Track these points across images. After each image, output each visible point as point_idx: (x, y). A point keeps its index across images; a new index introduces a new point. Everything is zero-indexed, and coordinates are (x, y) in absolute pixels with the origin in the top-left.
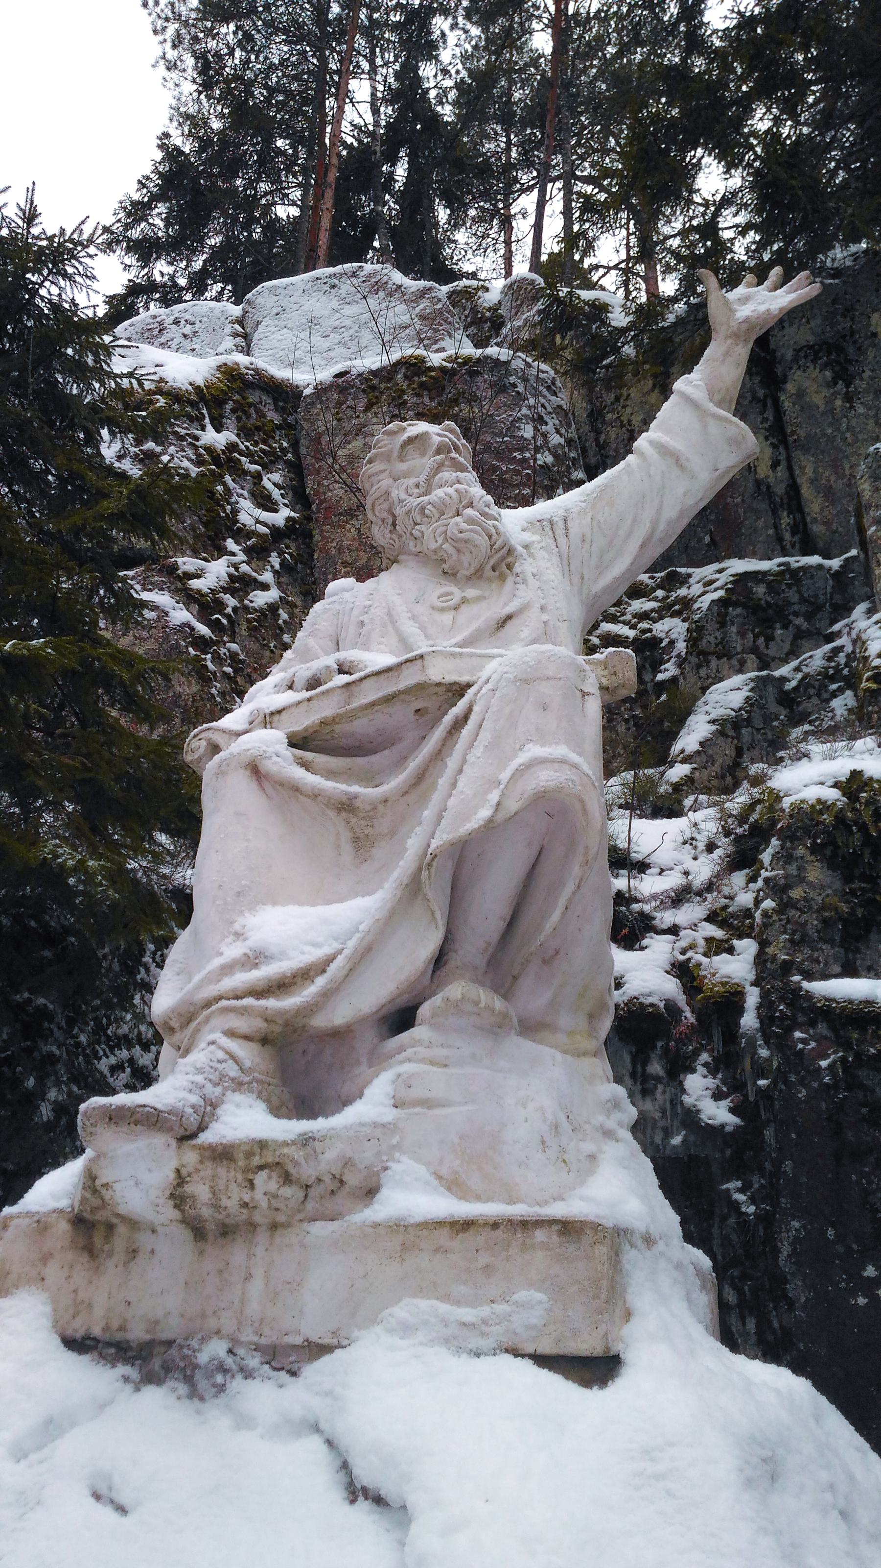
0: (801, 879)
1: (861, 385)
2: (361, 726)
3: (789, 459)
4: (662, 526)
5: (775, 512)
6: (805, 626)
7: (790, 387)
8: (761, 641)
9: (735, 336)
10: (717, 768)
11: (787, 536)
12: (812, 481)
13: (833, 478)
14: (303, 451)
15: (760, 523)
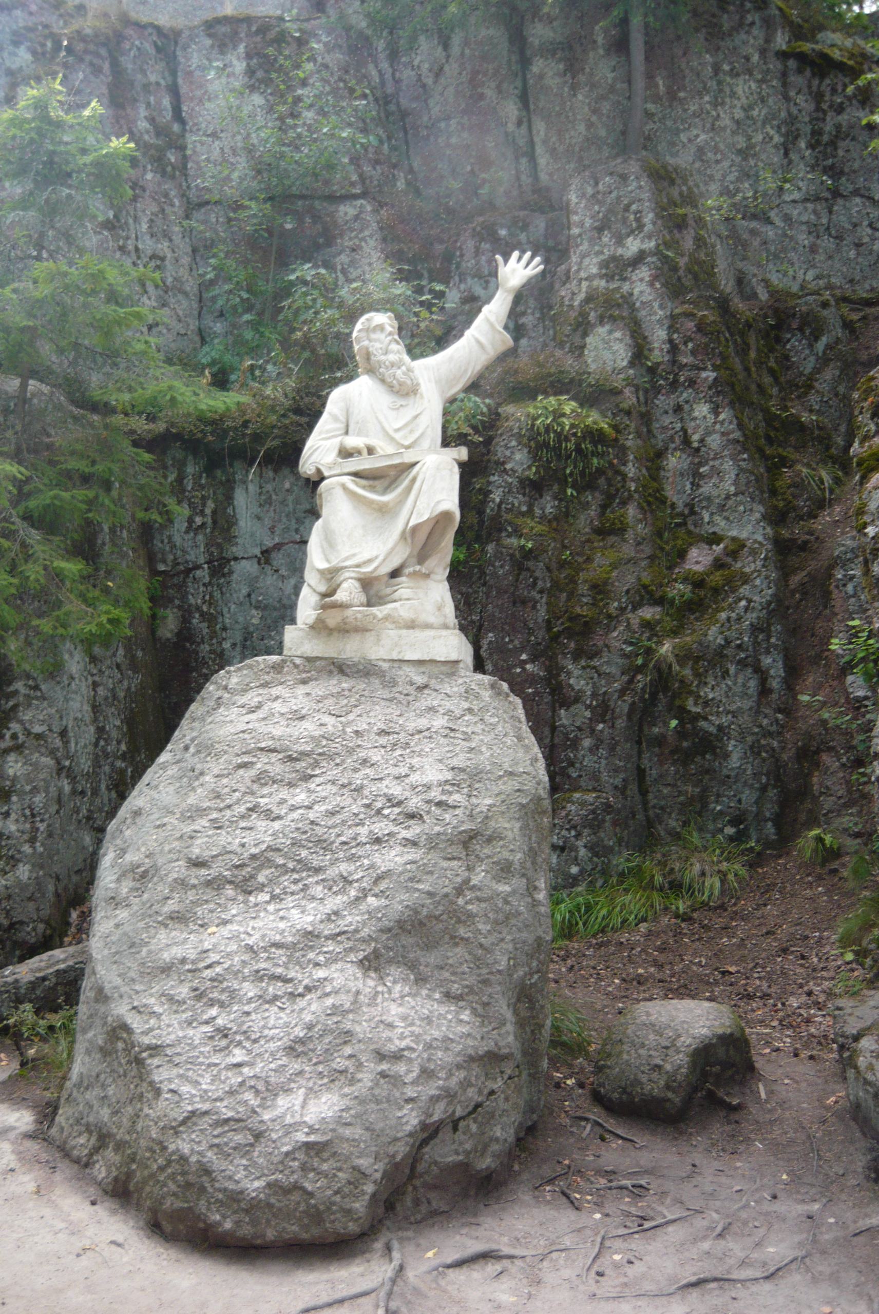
1: (582, 78)
3: (529, 121)
5: (517, 158)
7: (535, 69)
9: (508, 291)
11: (523, 177)
14: (180, 81)
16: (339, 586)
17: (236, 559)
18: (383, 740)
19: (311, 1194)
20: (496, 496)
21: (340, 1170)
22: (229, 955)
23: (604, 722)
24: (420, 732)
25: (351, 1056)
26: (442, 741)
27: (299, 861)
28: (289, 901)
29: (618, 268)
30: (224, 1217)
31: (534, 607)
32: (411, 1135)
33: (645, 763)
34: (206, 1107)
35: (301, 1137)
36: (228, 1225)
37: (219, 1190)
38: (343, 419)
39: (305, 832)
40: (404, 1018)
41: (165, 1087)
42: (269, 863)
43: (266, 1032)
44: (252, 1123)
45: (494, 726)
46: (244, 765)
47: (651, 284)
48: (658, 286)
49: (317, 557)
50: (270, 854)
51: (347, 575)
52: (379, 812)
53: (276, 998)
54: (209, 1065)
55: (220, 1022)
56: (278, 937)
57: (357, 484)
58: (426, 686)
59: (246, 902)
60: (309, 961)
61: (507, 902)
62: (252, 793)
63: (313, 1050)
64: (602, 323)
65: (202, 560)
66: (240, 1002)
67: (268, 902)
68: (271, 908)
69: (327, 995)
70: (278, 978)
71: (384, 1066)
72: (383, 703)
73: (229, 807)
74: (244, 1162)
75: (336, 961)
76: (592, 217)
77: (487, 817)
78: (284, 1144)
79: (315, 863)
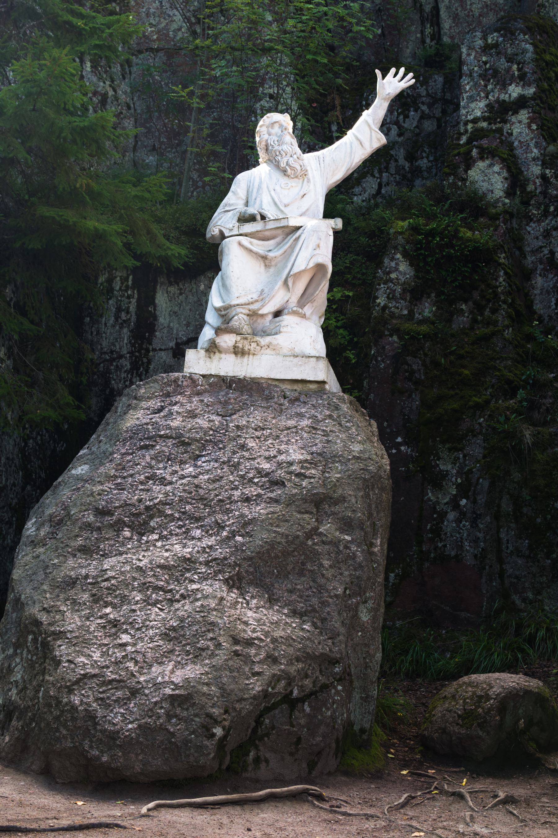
0: (396, 269)
2: (267, 233)
4: (354, 164)
5: (423, 23)
6: (427, 111)
8: (401, 117)
10: (366, 195)
11: (428, 40)
12: (448, 8)
13: (459, 9)
15: (413, 28)
16: (231, 319)
17: (154, 350)
18: (258, 434)
19: (173, 734)
20: (381, 301)
21: (196, 715)
22: (122, 573)
23: (467, 498)
24: (289, 428)
25: (212, 639)
26: (305, 435)
27: (184, 513)
28: (174, 540)
29: (501, 111)
30: (102, 752)
31: (410, 396)
32: (255, 697)
33: (502, 535)
34: (97, 671)
35: (168, 691)
36: (105, 759)
37: (101, 731)
38: (244, 198)
39: (191, 493)
40: (258, 621)
41: (64, 659)
42: (161, 513)
43: (148, 623)
44: (132, 683)
45: (349, 428)
46: (146, 447)
47: (529, 127)
48: (534, 127)
49: (215, 300)
50: (160, 507)
51: (239, 310)
52: (251, 480)
53: (157, 602)
54: (100, 645)
55: (112, 616)
56: (162, 561)
57: (251, 243)
58: (297, 399)
59: (139, 541)
60: (186, 578)
61: (346, 547)
62: (151, 467)
63: (183, 636)
64: (482, 159)
65: (124, 351)
66: (129, 603)
67: (157, 540)
68: (159, 544)
69: (197, 600)
70: (161, 589)
71: (238, 648)
72: (261, 409)
73: (131, 476)
74: (122, 711)
75: (206, 579)
76: (480, 67)
77: (335, 485)
78: (153, 697)
79: (197, 514)
